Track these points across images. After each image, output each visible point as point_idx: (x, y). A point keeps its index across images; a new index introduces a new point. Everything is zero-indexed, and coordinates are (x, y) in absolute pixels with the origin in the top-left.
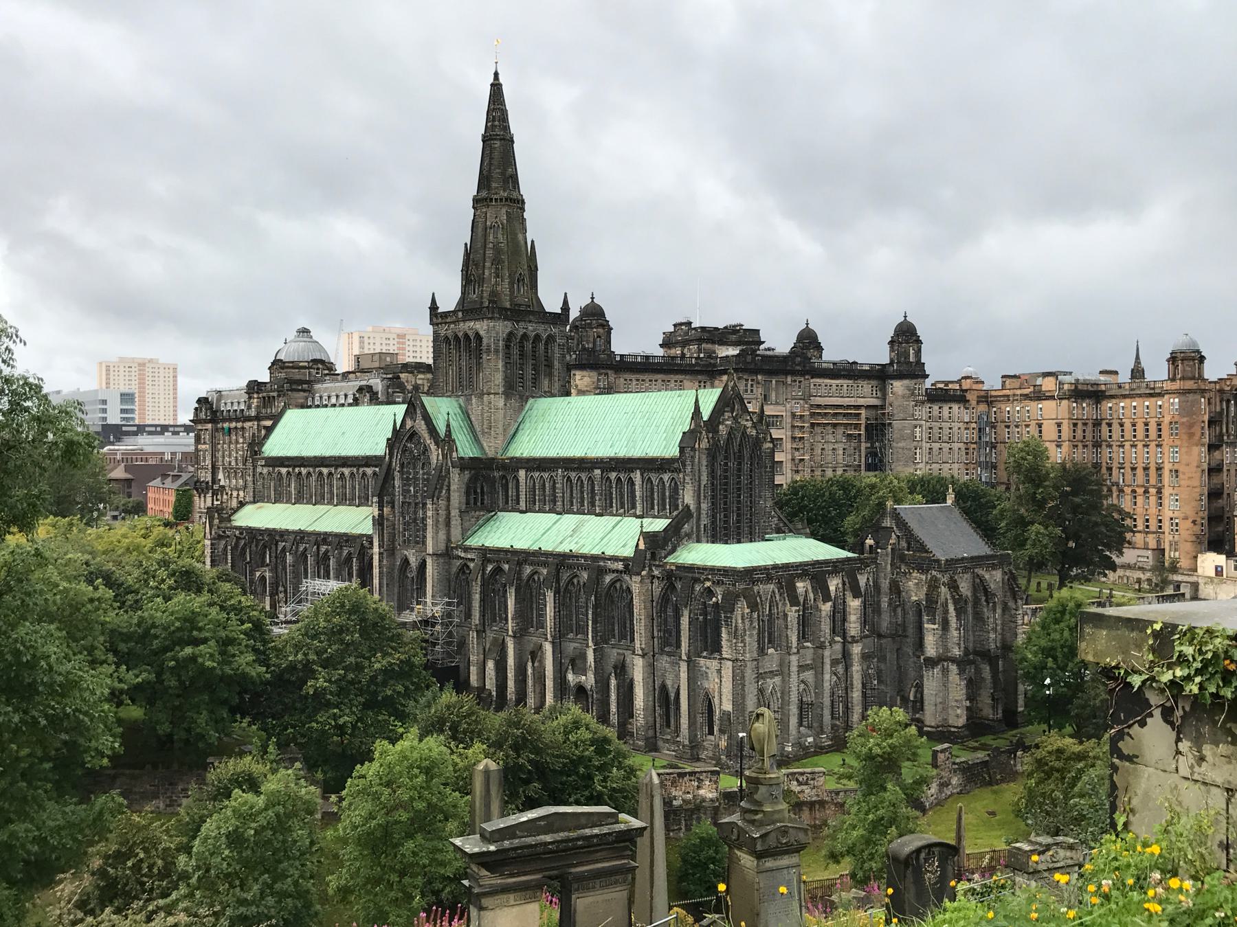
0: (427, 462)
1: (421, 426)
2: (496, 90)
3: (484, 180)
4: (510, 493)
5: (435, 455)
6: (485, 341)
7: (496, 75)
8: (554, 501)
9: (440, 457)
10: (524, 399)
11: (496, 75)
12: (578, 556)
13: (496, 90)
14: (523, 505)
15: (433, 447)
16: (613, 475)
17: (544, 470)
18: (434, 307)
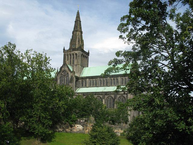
0: (68, 76)
1: (66, 69)
2: (78, 14)
3: (76, 27)
4: (84, 84)
5: (70, 75)
6: (78, 55)
7: (78, 11)
8: (96, 85)
9: (72, 75)
10: (83, 67)
11: (78, 11)
12: (110, 92)
13: (78, 14)
14: (87, 86)
15: (70, 73)
16: (112, 78)
17: (94, 78)
18: (64, 49)
